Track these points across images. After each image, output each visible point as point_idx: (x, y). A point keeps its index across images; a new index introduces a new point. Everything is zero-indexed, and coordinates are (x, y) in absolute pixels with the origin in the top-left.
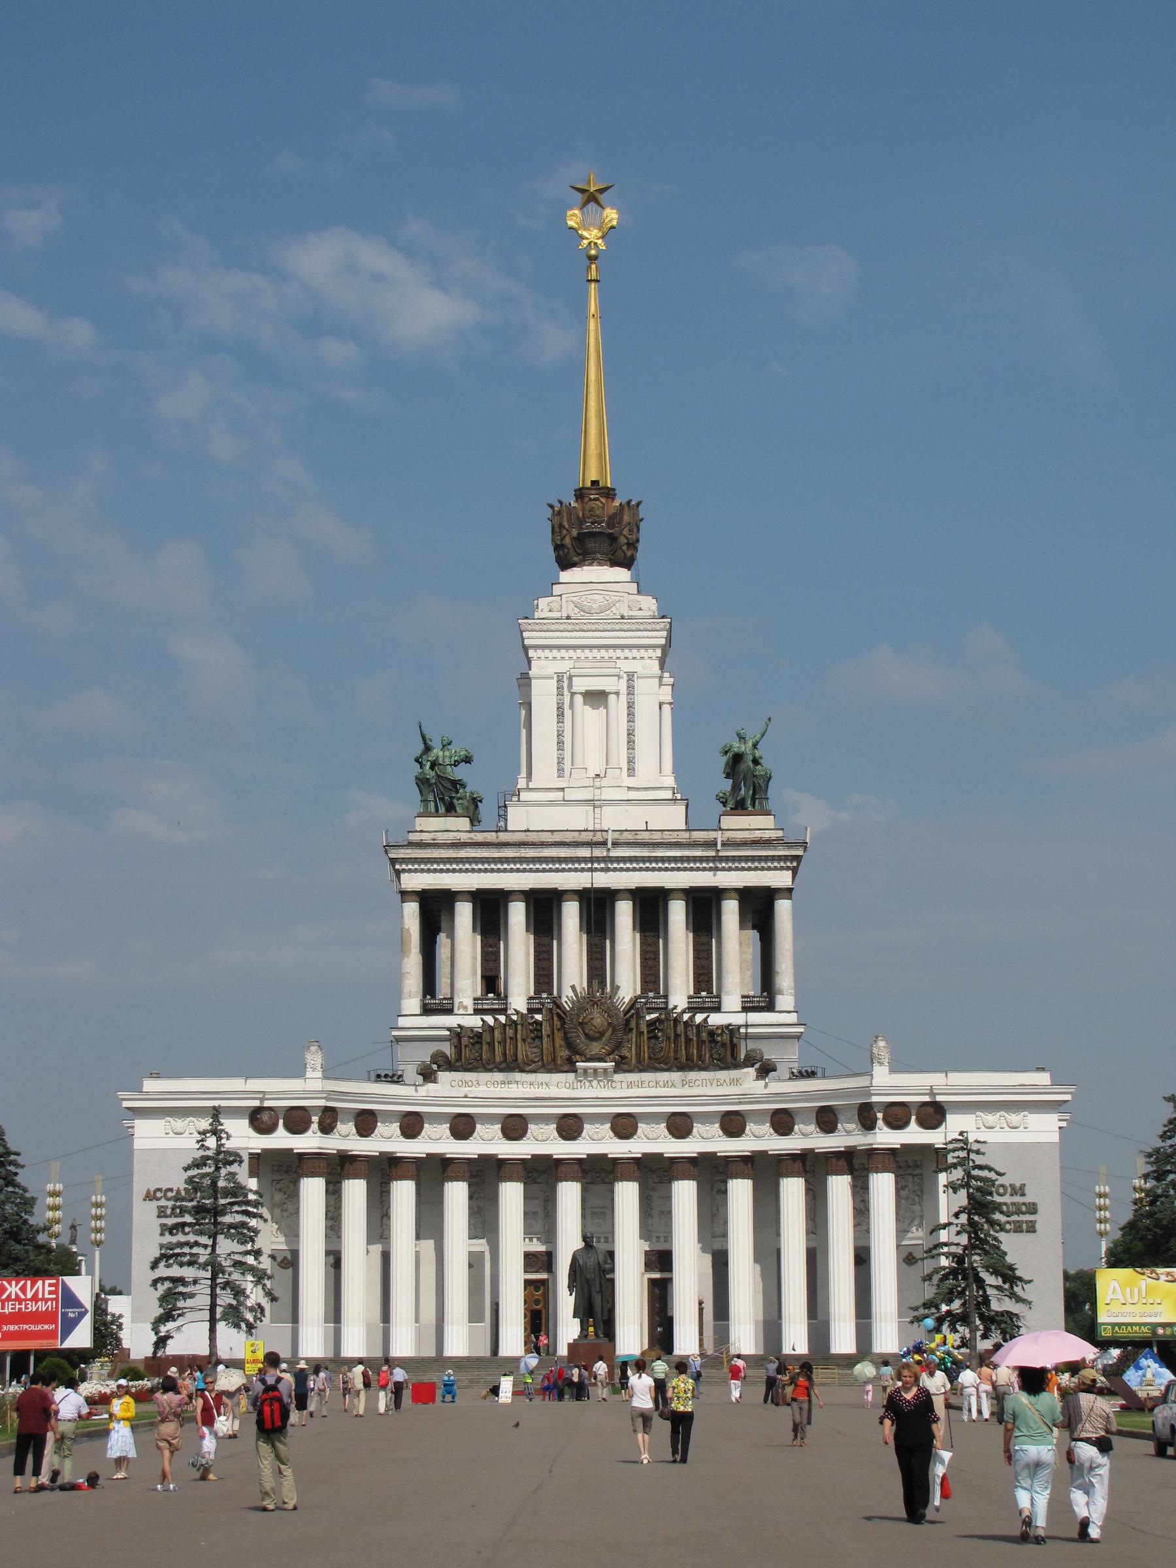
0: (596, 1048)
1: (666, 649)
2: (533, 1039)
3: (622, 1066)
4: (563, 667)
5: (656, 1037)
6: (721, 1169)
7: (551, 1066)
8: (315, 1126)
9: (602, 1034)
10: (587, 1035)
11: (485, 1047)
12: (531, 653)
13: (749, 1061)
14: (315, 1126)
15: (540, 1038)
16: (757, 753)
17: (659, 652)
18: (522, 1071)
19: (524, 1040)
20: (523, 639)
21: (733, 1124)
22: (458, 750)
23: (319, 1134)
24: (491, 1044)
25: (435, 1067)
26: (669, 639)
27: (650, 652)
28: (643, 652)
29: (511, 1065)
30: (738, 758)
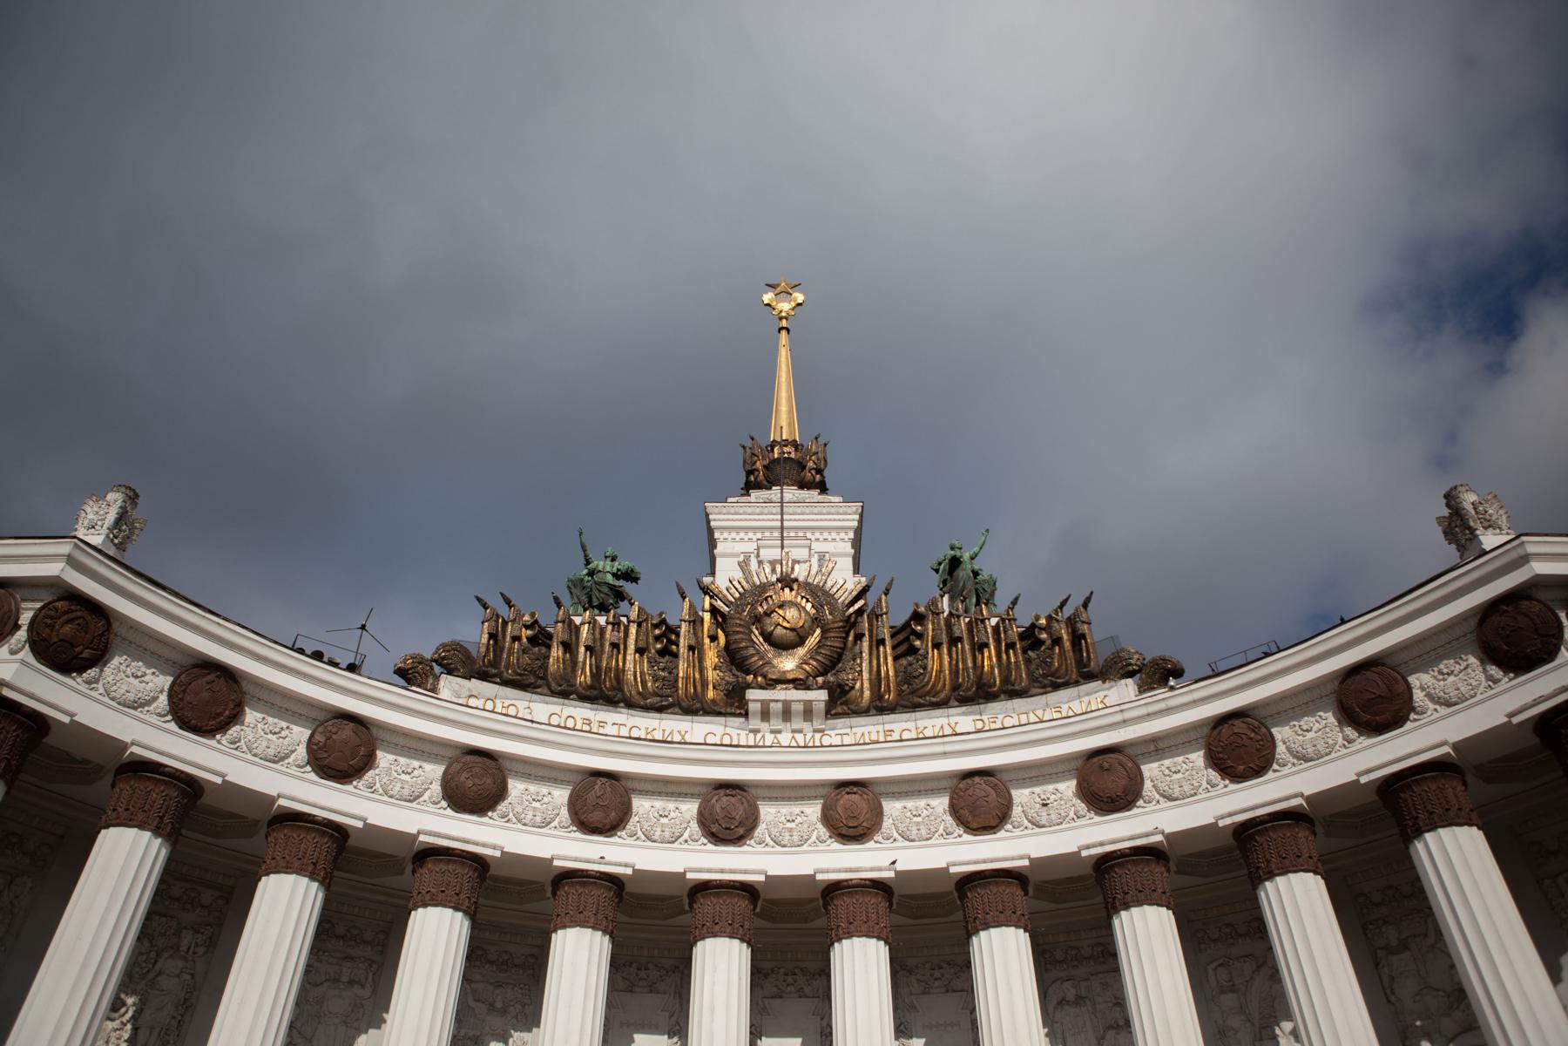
0: (788, 664)
1: (858, 532)
2: (662, 653)
3: (841, 703)
4: (751, 547)
5: (913, 651)
6: (1059, 955)
7: (694, 707)
8: (22, 634)
9: (801, 641)
10: (768, 637)
11: (556, 652)
12: (717, 535)
13: (1116, 668)
14: (22, 634)
15: (676, 656)
16: (976, 568)
17: (851, 535)
18: (630, 705)
19: (640, 651)
20: (708, 522)
21: (1108, 780)
22: (623, 564)
23: (26, 654)
24: (568, 647)
25: (437, 669)
26: (861, 521)
27: (842, 535)
28: (834, 535)
29: (606, 692)
30: (955, 563)
